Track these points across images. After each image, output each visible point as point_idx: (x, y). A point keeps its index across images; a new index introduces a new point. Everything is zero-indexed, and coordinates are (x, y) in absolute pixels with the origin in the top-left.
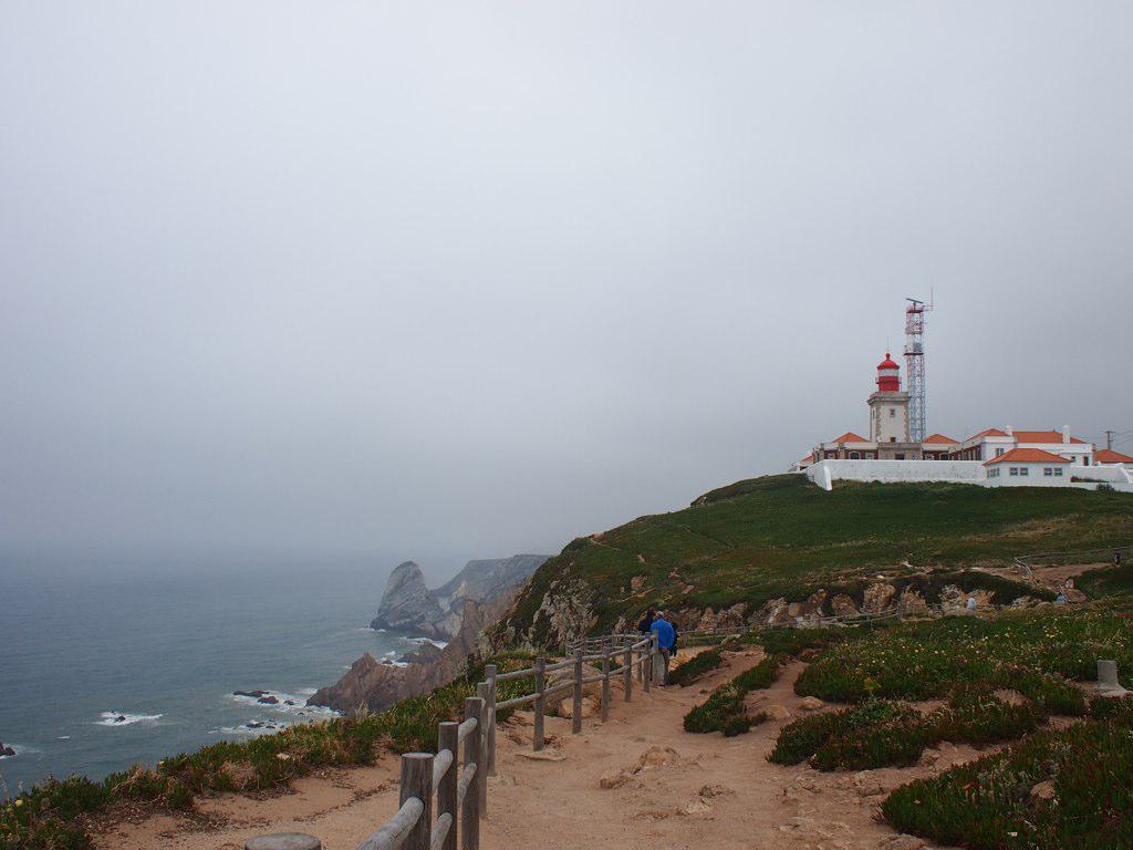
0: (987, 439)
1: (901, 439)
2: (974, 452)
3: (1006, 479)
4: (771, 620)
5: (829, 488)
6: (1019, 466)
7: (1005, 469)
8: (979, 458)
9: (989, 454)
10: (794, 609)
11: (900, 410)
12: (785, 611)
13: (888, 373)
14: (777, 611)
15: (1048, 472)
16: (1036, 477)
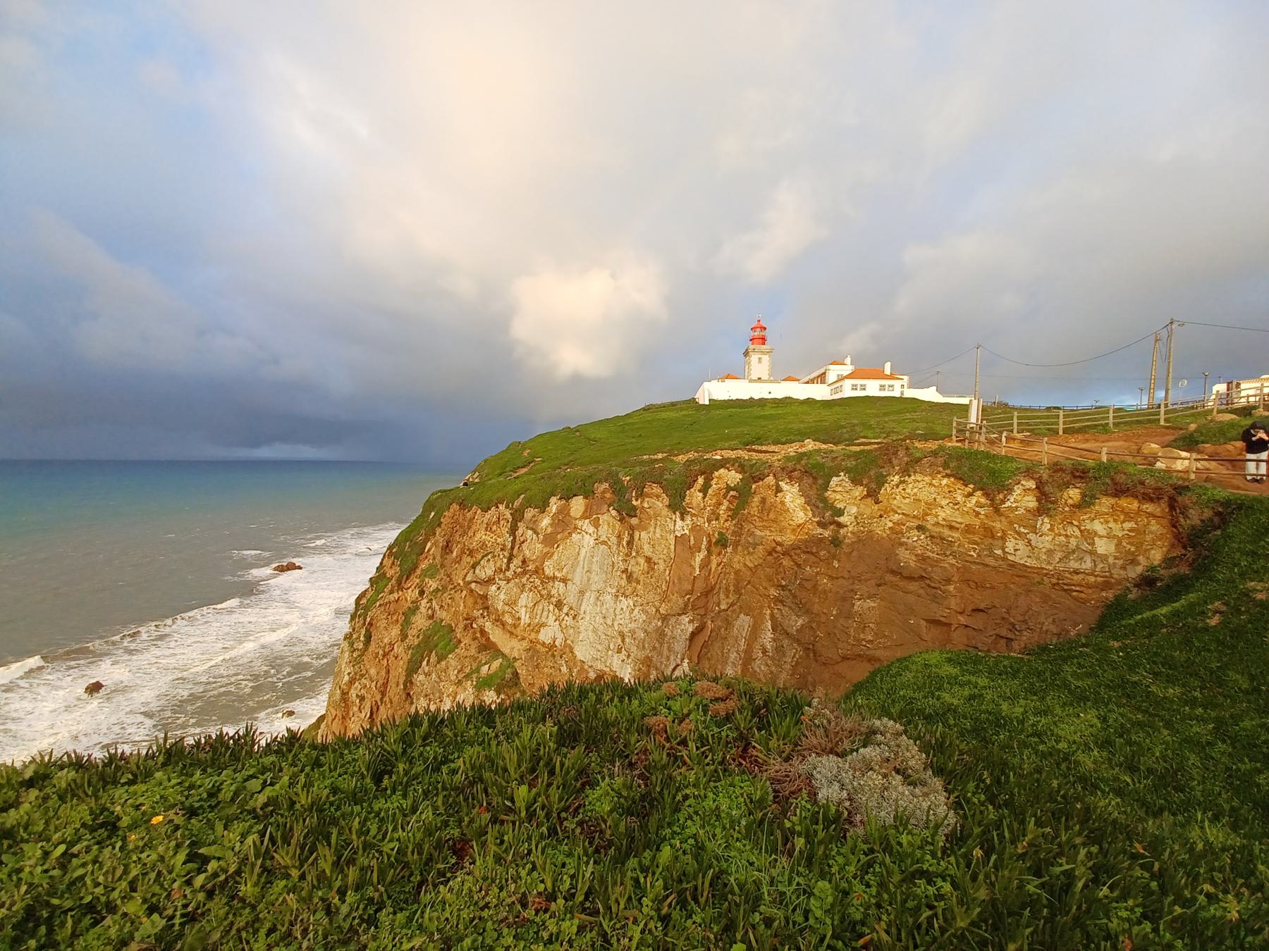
0: (831, 367)
1: (765, 377)
2: (822, 378)
3: (847, 392)
4: (545, 522)
5: (707, 403)
6: (859, 382)
7: (848, 384)
8: (823, 382)
9: (832, 377)
10: (578, 505)
11: (766, 358)
12: (564, 511)
13: (757, 333)
14: (554, 508)
15: (882, 388)
16: (873, 388)
